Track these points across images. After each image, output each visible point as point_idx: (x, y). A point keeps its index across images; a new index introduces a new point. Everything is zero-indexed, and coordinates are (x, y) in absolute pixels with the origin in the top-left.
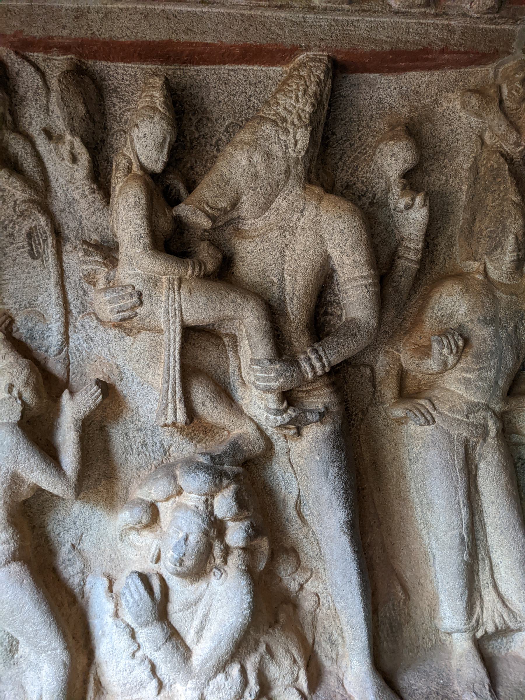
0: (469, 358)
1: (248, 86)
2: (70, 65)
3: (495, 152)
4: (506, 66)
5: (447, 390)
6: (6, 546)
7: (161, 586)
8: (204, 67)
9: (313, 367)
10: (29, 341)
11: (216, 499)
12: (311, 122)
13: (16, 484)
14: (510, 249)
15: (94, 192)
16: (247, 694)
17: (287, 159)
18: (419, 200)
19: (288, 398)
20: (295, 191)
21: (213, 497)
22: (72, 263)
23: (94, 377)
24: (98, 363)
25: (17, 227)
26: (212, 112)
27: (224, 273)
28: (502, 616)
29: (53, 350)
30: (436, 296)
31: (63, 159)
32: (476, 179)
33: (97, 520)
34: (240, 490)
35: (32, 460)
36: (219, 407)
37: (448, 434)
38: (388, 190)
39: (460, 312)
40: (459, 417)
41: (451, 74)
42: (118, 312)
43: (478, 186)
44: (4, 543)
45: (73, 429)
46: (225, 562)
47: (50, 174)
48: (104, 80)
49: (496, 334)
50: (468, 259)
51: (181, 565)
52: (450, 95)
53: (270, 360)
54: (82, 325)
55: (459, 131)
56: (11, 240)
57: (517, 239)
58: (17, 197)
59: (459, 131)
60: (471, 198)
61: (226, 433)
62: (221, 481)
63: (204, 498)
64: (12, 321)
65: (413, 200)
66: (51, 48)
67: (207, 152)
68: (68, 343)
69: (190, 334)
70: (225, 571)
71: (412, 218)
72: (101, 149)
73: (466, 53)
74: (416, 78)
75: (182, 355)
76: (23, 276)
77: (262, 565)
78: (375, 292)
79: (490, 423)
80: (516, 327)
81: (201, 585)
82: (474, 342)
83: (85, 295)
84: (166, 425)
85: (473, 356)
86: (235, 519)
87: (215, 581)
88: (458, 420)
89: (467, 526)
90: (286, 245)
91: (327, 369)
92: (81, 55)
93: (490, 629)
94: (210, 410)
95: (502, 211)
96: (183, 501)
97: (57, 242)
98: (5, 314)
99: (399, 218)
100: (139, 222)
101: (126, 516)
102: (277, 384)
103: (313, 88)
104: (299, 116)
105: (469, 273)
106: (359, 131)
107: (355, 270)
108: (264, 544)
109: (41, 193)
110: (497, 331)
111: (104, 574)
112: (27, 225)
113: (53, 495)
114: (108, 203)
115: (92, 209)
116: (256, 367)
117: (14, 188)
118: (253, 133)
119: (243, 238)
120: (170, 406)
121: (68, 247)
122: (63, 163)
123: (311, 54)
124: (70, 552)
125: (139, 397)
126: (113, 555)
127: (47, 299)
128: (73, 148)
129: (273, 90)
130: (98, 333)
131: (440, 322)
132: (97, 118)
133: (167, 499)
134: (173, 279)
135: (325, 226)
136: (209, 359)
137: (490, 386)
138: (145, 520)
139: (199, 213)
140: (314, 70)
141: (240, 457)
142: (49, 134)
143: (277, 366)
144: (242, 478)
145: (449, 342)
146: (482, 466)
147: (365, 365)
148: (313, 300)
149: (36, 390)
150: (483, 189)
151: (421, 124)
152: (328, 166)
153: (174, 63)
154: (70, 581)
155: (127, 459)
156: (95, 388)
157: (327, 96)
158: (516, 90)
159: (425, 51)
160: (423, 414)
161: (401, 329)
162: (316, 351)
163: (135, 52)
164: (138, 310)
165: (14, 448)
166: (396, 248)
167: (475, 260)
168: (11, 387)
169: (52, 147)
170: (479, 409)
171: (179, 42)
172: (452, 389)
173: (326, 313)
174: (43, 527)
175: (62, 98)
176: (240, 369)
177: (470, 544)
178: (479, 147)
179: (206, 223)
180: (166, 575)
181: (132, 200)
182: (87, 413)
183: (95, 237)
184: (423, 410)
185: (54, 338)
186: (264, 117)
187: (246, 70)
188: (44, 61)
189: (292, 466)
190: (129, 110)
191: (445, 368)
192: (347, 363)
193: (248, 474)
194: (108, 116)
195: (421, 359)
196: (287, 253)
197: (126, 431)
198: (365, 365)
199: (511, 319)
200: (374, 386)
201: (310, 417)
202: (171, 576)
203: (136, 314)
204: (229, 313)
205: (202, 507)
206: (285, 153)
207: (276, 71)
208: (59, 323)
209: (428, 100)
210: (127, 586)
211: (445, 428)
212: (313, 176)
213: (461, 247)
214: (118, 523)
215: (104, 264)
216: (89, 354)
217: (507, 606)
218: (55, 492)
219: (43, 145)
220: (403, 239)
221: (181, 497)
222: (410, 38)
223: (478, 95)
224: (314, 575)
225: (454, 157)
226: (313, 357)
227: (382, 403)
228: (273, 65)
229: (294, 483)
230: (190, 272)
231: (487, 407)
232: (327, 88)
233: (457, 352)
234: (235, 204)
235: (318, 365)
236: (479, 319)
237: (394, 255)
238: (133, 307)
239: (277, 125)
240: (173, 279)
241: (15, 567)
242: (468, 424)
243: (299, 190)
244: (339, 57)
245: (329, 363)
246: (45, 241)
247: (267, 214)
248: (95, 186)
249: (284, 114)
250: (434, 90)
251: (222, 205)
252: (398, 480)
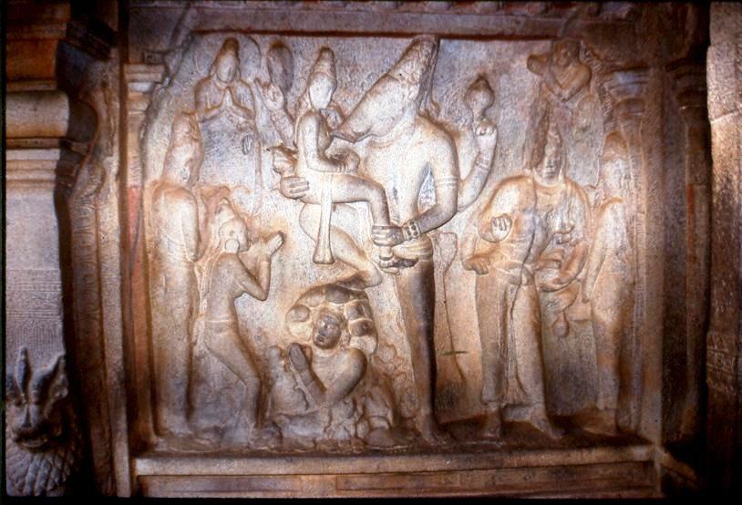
16: (356, 415)
28: (518, 395)
41: (522, 44)
65: (485, 130)
79: (523, 276)
80: (547, 216)
93: (511, 402)
132: (289, 71)
201: (406, 263)
217: (523, 391)
222: (489, 27)
226: (410, 227)
231: (522, 266)
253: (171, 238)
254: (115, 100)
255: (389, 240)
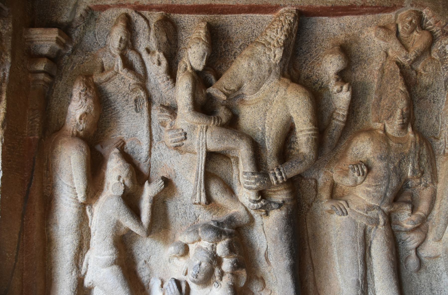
0: (370, 179)
1: (253, 25)
2: (161, 17)
3: (394, 61)
4: (402, 13)
5: (357, 196)
6: (112, 257)
7: (186, 287)
8: (230, 15)
9: (276, 178)
10: (132, 154)
11: (218, 245)
12: (284, 45)
13: (118, 226)
14: (398, 117)
15: (168, 80)
17: (269, 64)
18: (345, 87)
19: (262, 194)
20: (274, 81)
21: (217, 244)
22: (156, 115)
23: (161, 175)
24: (164, 168)
25: (130, 97)
26: (233, 38)
27: (232, 124)
29: (143, 160)
30: (354, 142)
31: (154, 63)
32: (382, 76)
33: (158, 250)
34: (231, 242)
35: (127, 215)
36: (225, 196)
37: (354, 221)
38: (328, 81)
39: (368, 152)
40: (362, 212)
41: (370, 17)
42: (174, 142)
43: (383, 80)
44: (111, 255)
45: (148, 201)
46: (221, 279)
47: (148, 70)
48: (178, 23)
49: (387, 167)
50: (376, 121)
51: (196, 278)
52: (369, 29)
53: (252, 173)
54: (158, 148)
55: (374, 48)
56: (127, 103)
57: (402, 112)
58: (131, 82)
59: (374, 48)
60: (380, 86)
61: (229, 210)
62: (221, 236)
63: (211, 244)
64: (124, 143)
65: (342, 87)
66: (152, 9)
67: (229, 59)
68: (151, 156)
69: (211, 156)
70: (221, 284)
71: (342, 98)
72: (174, 57)
73: (376, 7)
74: (349, 20)
75: (206, 167)
76: (132, 121)
77: (242, 284)
78: (315, 139)
79: (381, 217)
80: (400, 162)
81: (207, 290)
82: (374, 170)
83: (161, 132)
84: (195, 204)
85: (373, 178)
86: (228, 256)
87: (215, 289)
88: (361, 214)
89: (362, 275)
90: (267, 110)
91: (285, 180)
92: (167, 11)
94: (219, 196)
95: (395, 95)
96: (201, 245)
97: (149, 104)
98: (121, 140)
99: (335, 96)
100: (187, 97)
101: (172, 249)
102: (255, 186)
103: (286, 27)
104: (278, 42)
105: (375, 130)
106: (315, 47)
107: (304, 125)
108: (243, 274)
109: (143, 80)
110: (388, 165)
111: (160, 278)
112: (134, 96)
113: (137, 234)
114: (175, 85)
115: (167, 88)
116: (245, 176)
117: (130, 77)
118: (251, 51)
119: (245, 105)
120: (198, 194)
121: (154, 107)
122: (154, 65)
123: (287, 9)
124: (143, 265)
125: (184, 187)
126: (165, 269)
127: (142, 133)
128: (159, 58)
129: (267, 26)
130: (166, 152)
131: (356, 157)
132: (173, 42)
133: (193, 243)
134: (203, 126)
135: (289, 100)
136: (221, 170)
137: (381, 196)
138: (181, 253)
139: (219, 92)
140: (287, 17)
141: (233, 224)
142: (148, 51)
143: (256, 176)
144: (234, 236)
145: (358, 169)
146: (374, 242)
147: (312, 179)
148: (281, 141)
149: (132, 180)
150: (386, 82)
151: (351, 44)
152: (294, 67)
153: (214, 14)
154: (143, 279)
155: (176, 220)
156: (161, 181)
157: (295, 30)
158: (406, 27)
159: (352, 6)
160: (341, 209)
161: (335, 159)
162: (279, 170)
163: (193, 9)
164: (184, 142)
165: (119, 208)
166: (333, 113)
167: (380, 122)
168: (119, 177)
169: (149, 57)
170: (374, 209)
171: (215, 5)
172: (360, 196)
173: (290, 148)
174: (131, 250)
175: (155, 34)
176: (239, 176)
177: (363, 286)
178: (385, 58)
179: (224, 97)
180: (190, 283)
181: (185, 85)
182: (156, 193)
183: (168, 102)
184: (341, 207)
185: (144, 153)
186: (258, 42)
187: (252, 16)
188: (149, 15)
189: (264, 232)
190: (189, 38)
191: (356, 184)
192: (300, 176)
193: (236, 235)
194: (179, 40)
195: (343, 177)
196: (268, 114)
197: (176, 205)
198: (312, 179)
199: (397, 158)
200: (317, 191)
201: (273, 206)
202: (192, 283)
203: (183, 144)
204: (232, 146)
205: (209, 249)
206: (269, 61)
207: (269, 17)
208: (147, 146)
209: (356, 31)
210: (169, 285)
211: (353, 218)
212: (286, 73)
213: (373, 114)
214: (168, 253)
215: (170, 117)
216: (160, 163)
218: (137, 232)
219: (145, 56)
220: (336, 109)
221: (200, 242)
223: (384, 30)
224: (272, 293)
225: (370, 63)
226: (277, 173)
227: (321, 201)
228: (267, 13)
229: (265, 241)
230: (212, 123)
231: (379, 208)
232: (295, 26)
233: (363, 175)
234: (240, 88)
235: (279, 177)
236: (378, 157)
237: (331, 117)
238: (182, 140)
239: (265, 46)
240: (203, 126)
241: (115, 267)
242: (367, 217)
243: (276, 80)
244: (303, 9)
245: (286, 177)
246: (143, 103)
247: (258, 93)
248: (169, 77)
249: (269, 40)
250: (359, 26)
251: (232, 88)
252: (327, 246)
253: (64, 181)
254: (7, 55)
255: (258, 184)
